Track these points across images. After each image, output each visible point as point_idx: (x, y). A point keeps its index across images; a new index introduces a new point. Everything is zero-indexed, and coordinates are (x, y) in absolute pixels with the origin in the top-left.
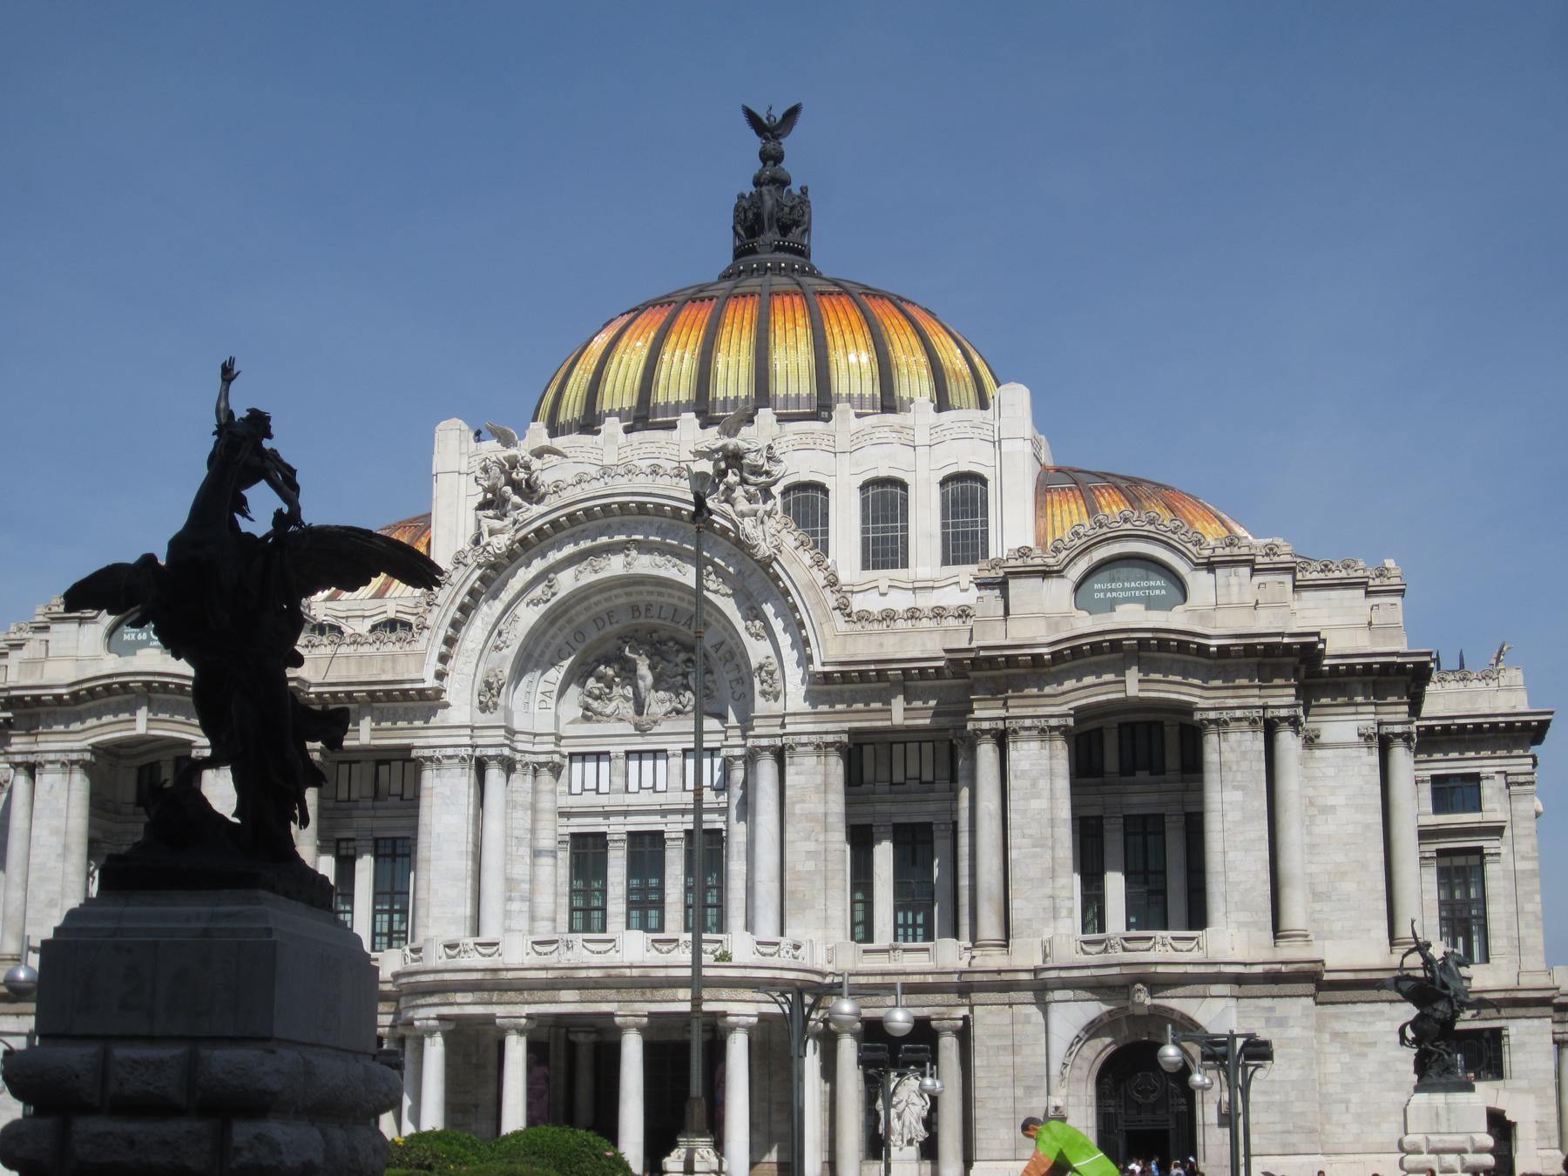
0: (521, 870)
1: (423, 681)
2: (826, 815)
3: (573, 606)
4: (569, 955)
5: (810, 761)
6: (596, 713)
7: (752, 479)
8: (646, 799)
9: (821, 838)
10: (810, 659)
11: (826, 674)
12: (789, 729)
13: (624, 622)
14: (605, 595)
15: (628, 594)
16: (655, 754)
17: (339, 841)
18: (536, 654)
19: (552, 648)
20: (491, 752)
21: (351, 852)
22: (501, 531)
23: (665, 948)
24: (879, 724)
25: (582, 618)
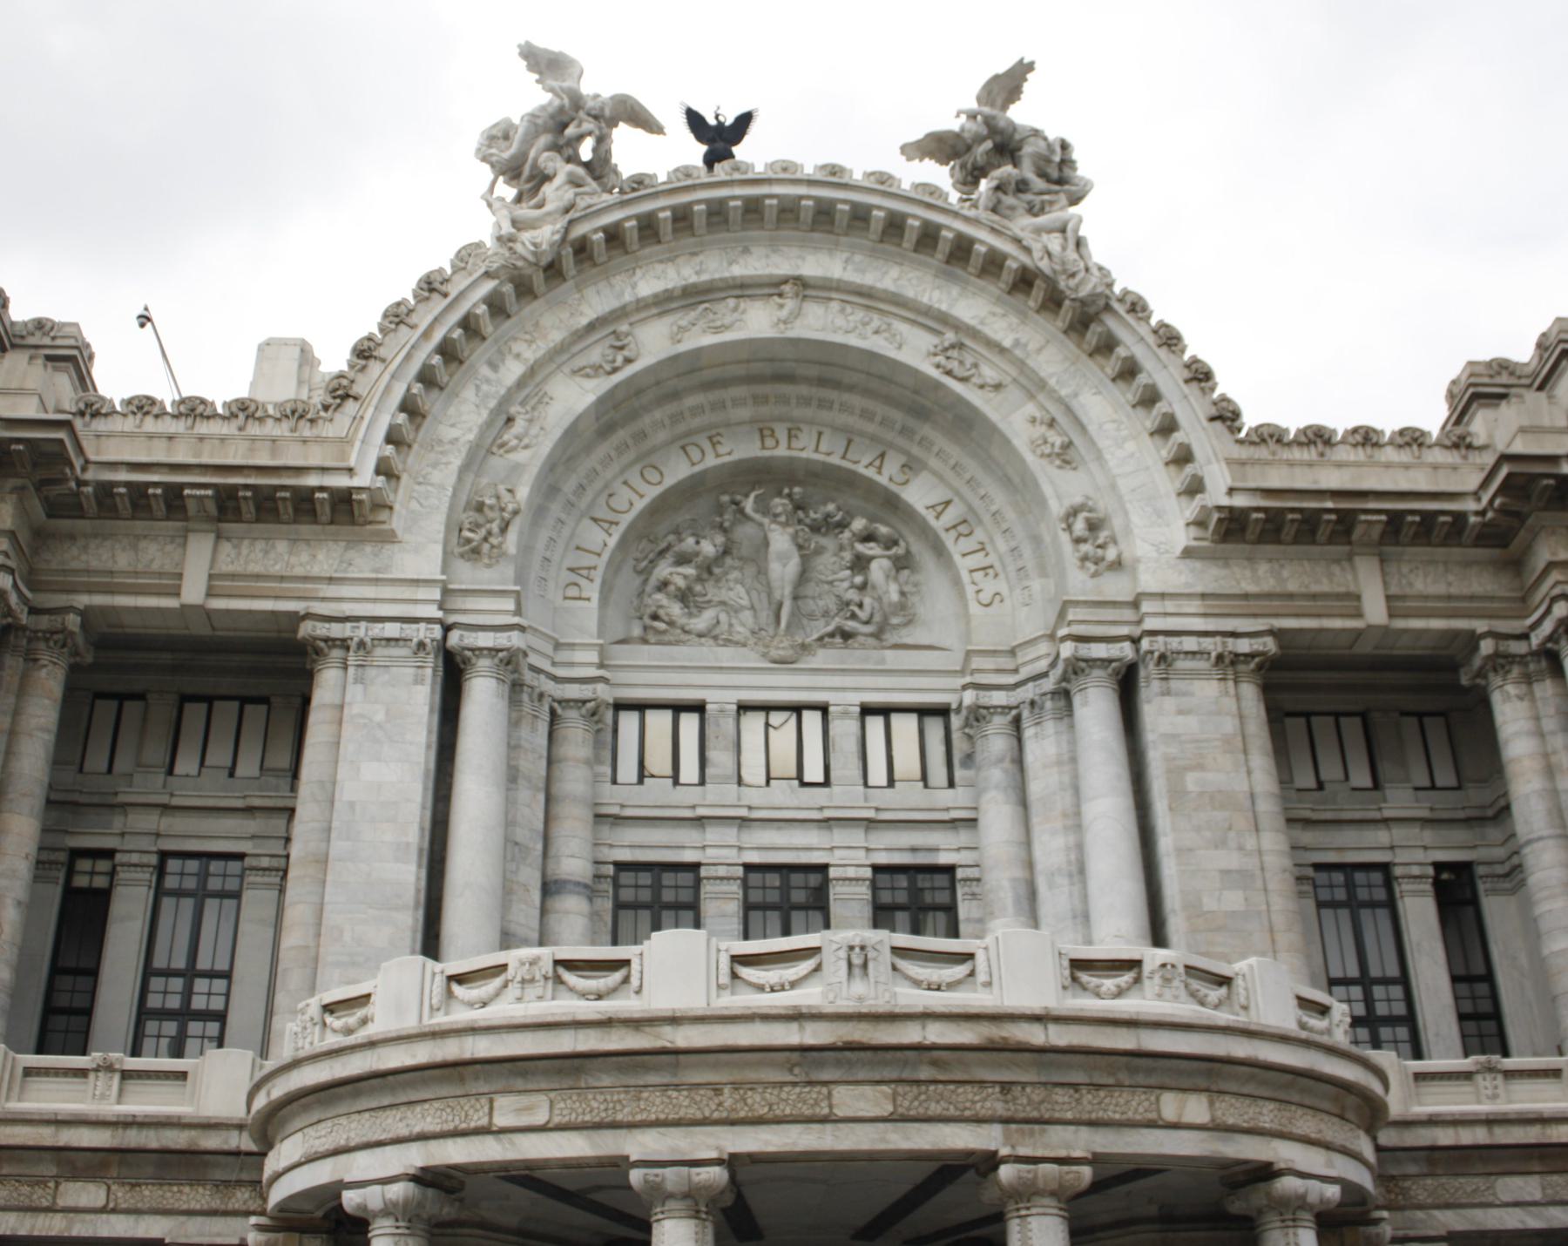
0: (526, 915)
1: (350, 471)
2: (1252, 796)
3: (646, 409)
4: (859, 987)
5: (1208, 690)
6: (671, 624)
7: (1039, 184)
8: (784, 796)
9: (1250, 843)
10: (1194, 488)
11: (1231, 509)
12: (1150, 624)
13: (743, 449)
14: (714, 395)
15: (759, 400)
16: (797, 709)
17: (78, 853)
18: (569, 486)
19: (598, 484)
20: (485, 640)
21: (100, 882)
22: (531, 225)
23: (1109, 984)
24: (1337, 623)
25: (662, 436)
